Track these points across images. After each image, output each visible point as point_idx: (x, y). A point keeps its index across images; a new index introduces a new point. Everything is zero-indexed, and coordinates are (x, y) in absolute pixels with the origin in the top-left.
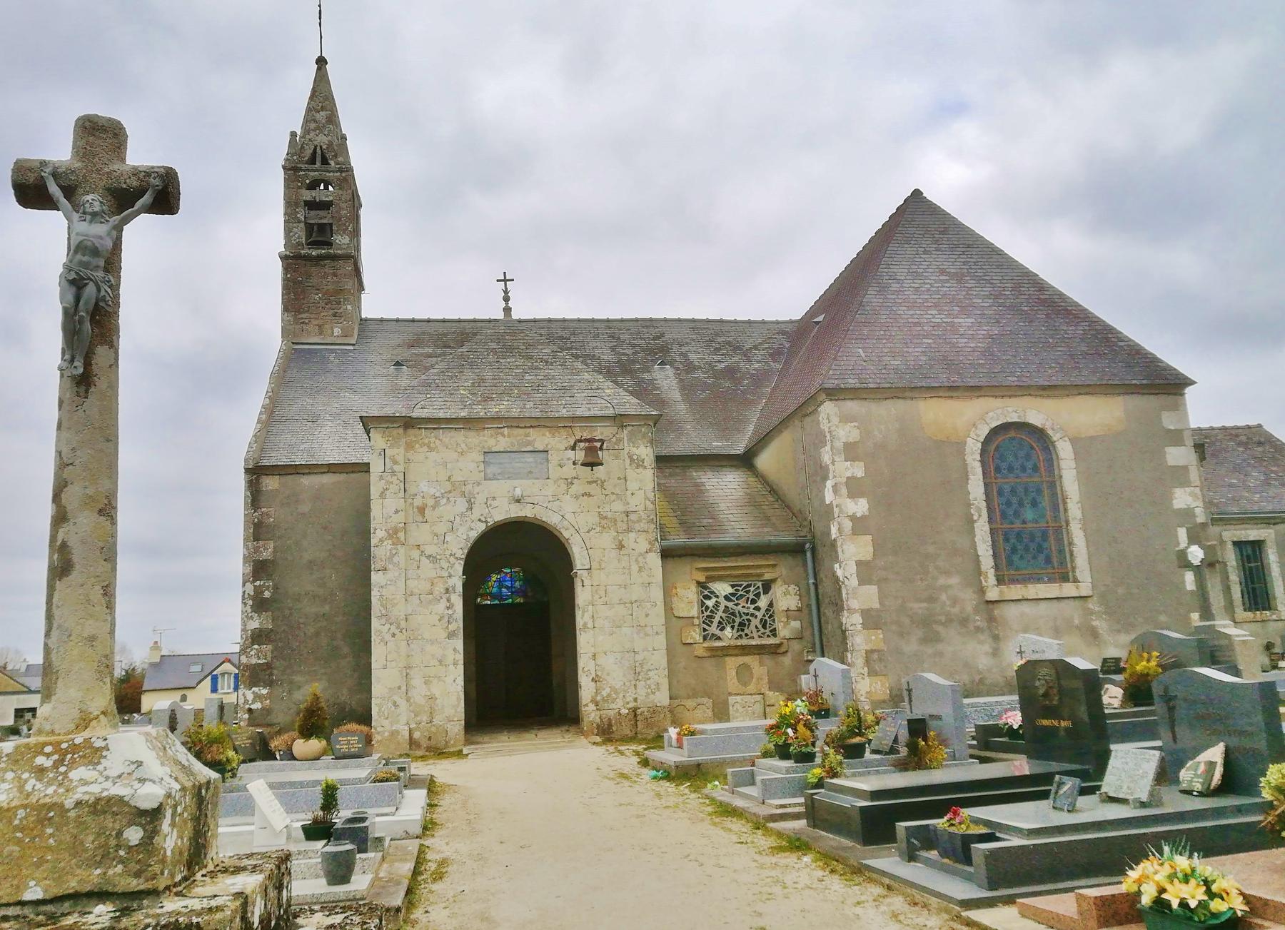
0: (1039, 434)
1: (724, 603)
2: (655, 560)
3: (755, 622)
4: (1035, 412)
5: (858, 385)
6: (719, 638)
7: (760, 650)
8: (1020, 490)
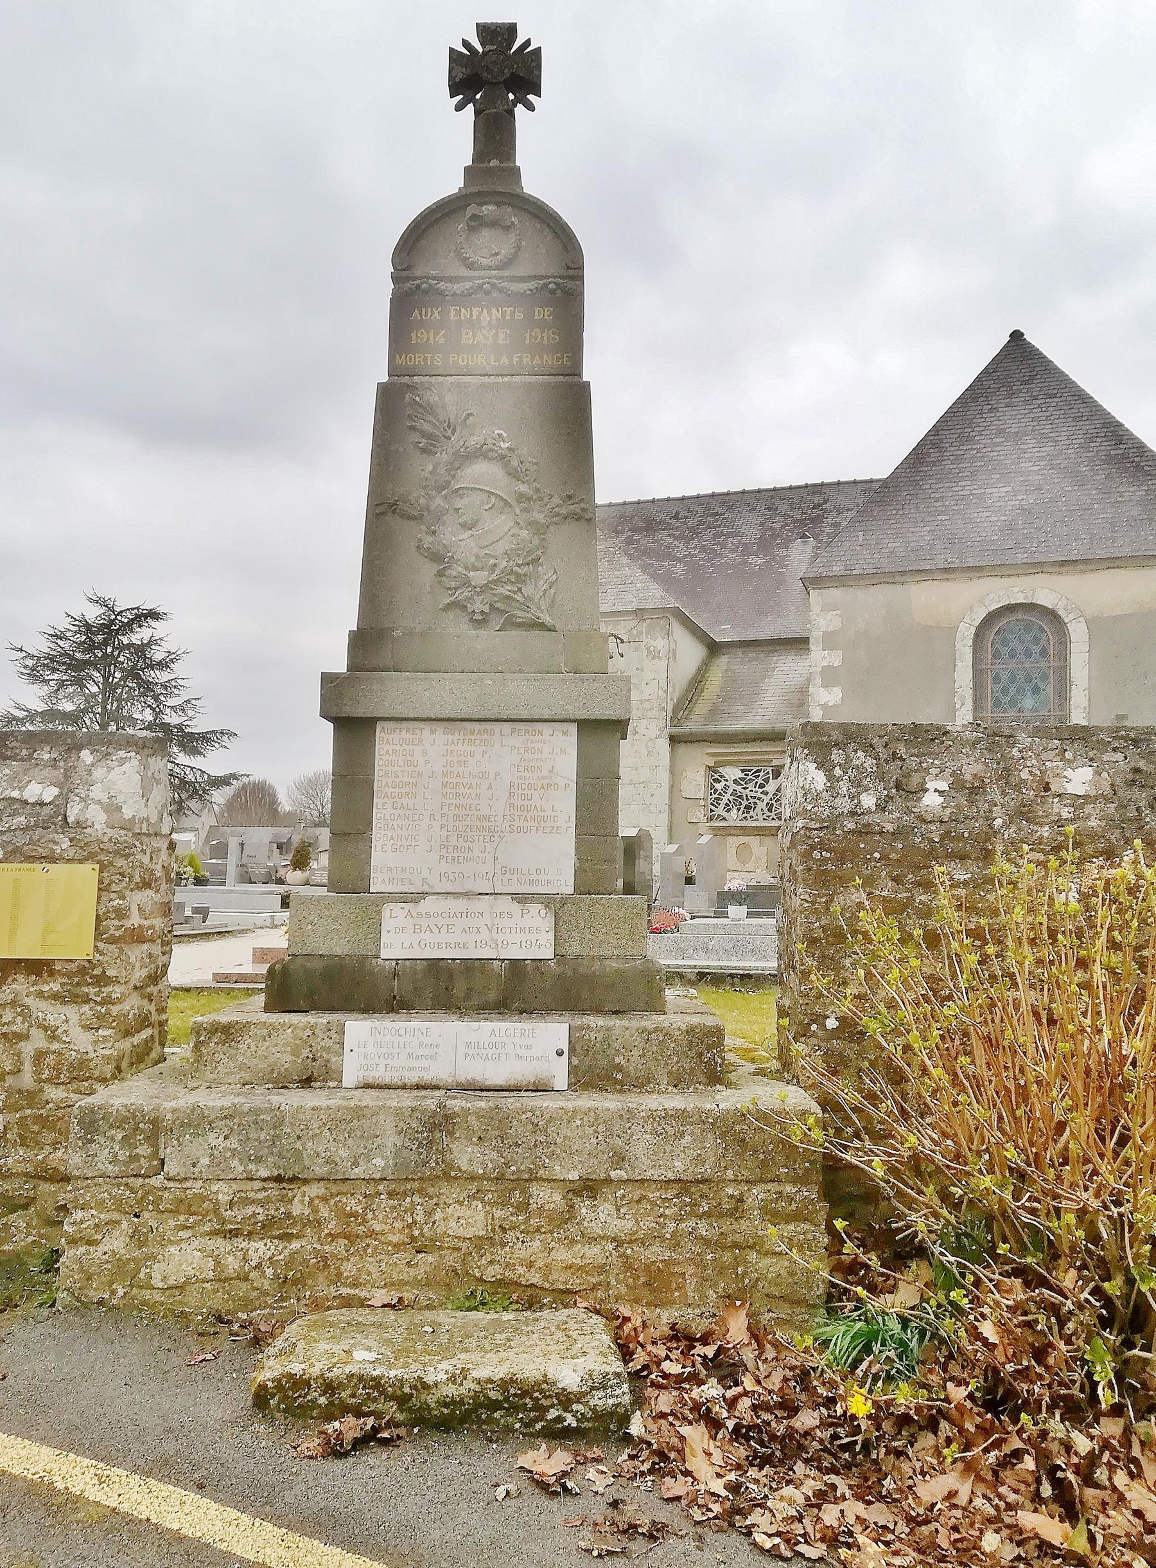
0: (1051, 615)
1: (733, 787)
2: (664, 745)
3: (761, 805)
4: (1045, 591)
5: (842, 573)
6: (725, 819)
7: (761, 832)
8: (1020, 676)
